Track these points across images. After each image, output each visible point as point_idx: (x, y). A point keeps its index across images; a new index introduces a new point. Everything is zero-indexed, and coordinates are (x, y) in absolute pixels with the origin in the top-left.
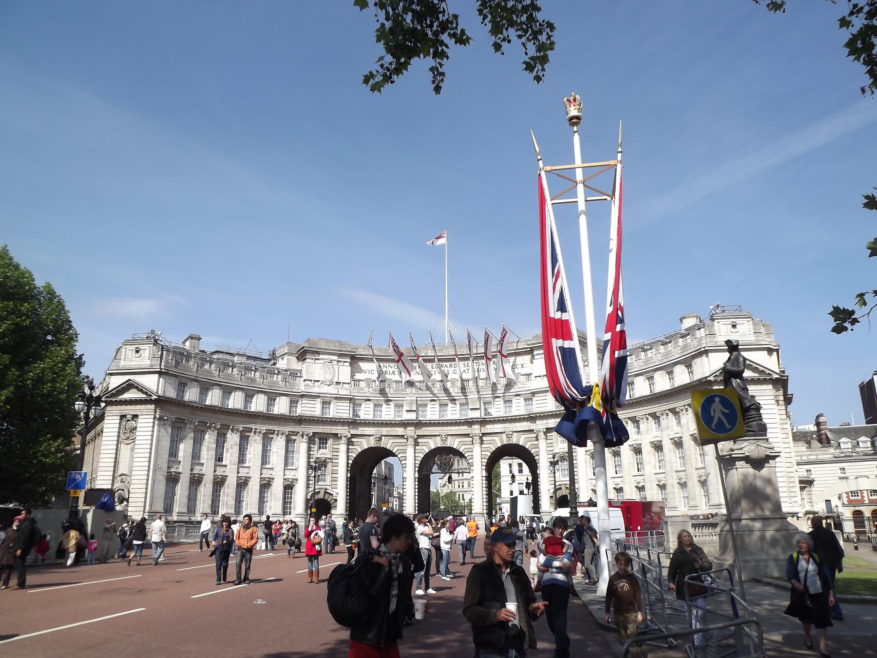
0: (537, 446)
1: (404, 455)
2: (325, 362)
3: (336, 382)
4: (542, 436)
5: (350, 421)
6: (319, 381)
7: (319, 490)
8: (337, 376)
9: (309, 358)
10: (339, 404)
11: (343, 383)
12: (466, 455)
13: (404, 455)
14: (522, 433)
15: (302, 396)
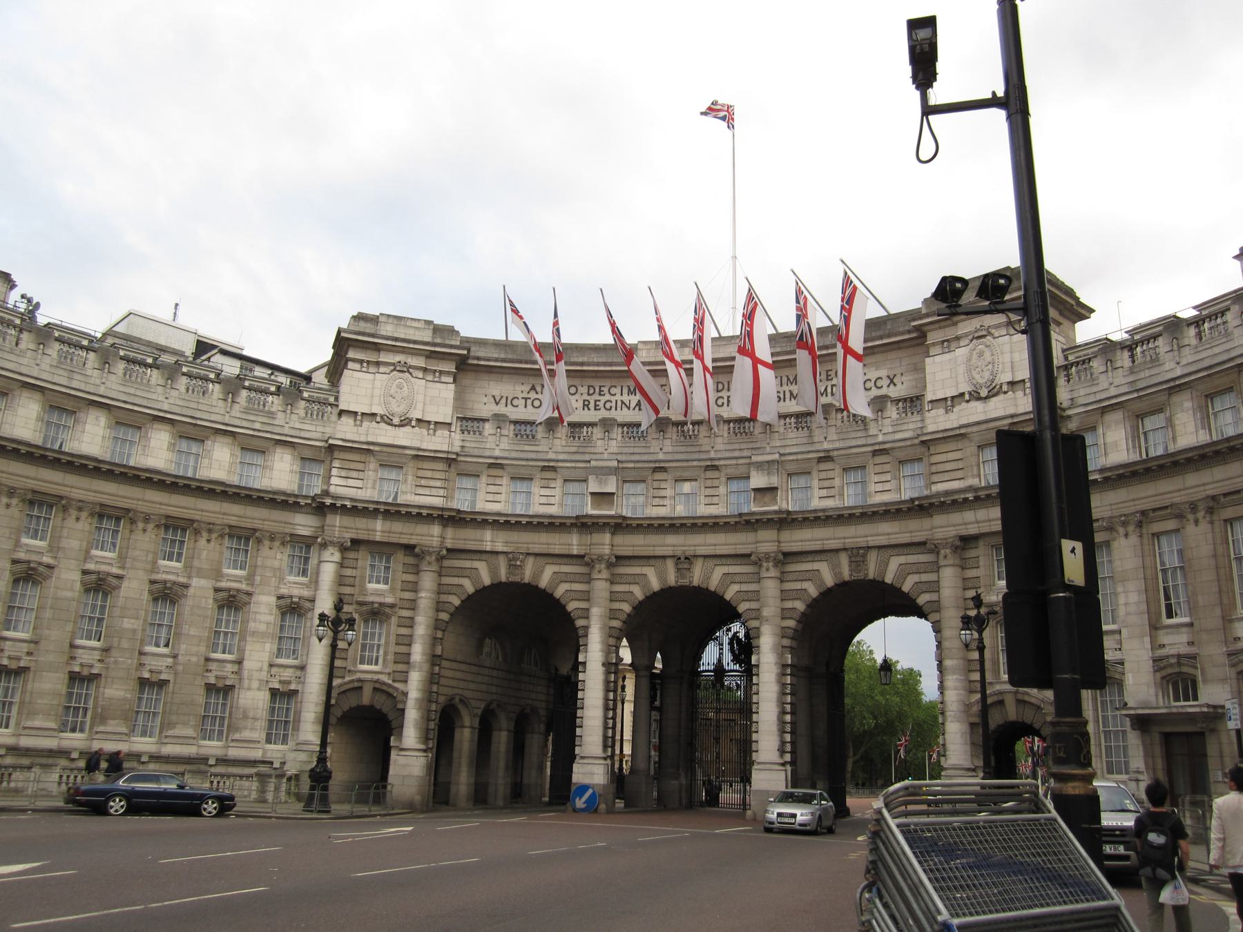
0: (935, 587)
1: (583, 605)
2: (395, 370)
3: (419, 420)
4: (948, 559)
5: (446, 514)
6: (374, 415)
7: (359, 684)
8: (420, 406)
9: (354, 360)
10: (421, 473)
11: (436, 423)
12: (742, 608)
13: (583, 605)
14: (891, 552)
15: (331, 448)
